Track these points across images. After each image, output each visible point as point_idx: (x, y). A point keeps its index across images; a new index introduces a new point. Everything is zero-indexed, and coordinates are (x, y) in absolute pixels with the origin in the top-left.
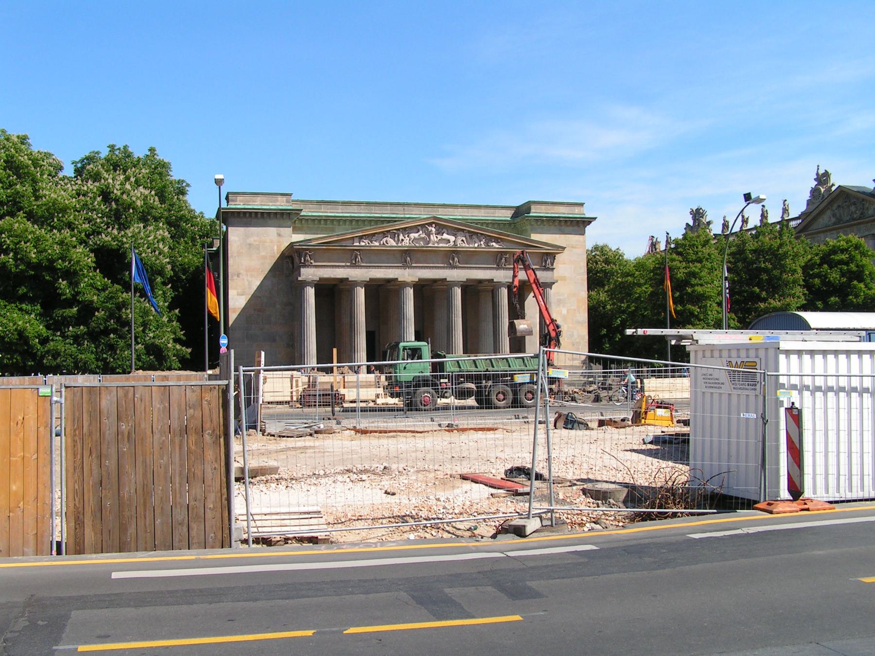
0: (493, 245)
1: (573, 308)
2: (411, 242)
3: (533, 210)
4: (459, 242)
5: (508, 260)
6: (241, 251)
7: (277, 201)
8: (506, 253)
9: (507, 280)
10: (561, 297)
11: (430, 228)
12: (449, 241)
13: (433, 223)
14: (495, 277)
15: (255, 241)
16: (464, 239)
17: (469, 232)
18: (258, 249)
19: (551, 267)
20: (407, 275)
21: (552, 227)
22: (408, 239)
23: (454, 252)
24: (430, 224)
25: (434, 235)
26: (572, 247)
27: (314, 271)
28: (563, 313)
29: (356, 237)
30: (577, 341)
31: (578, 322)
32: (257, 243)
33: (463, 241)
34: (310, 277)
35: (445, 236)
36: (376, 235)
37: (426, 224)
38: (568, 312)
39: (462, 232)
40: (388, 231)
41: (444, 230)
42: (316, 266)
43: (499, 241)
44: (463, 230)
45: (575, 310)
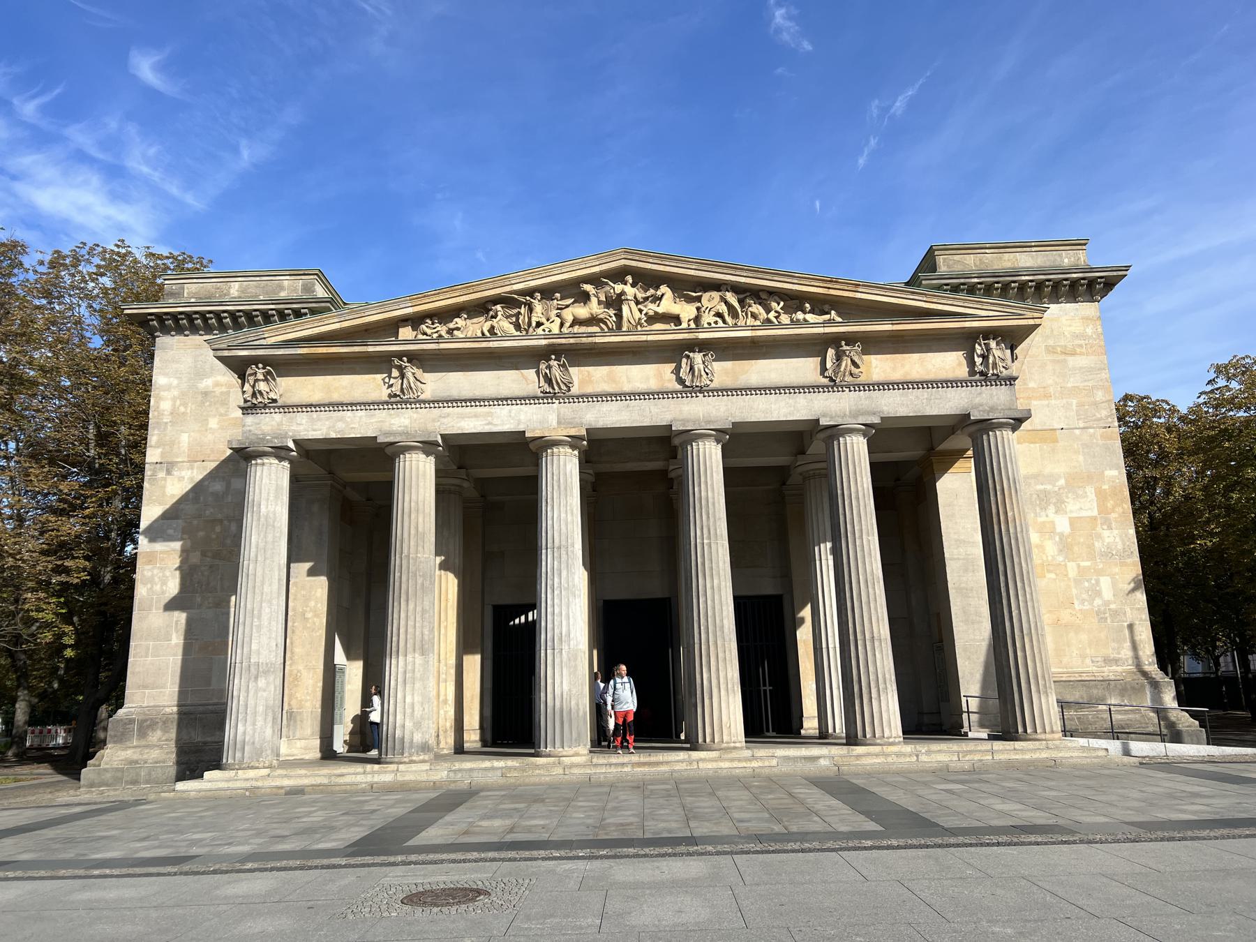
1: (1089, 514)
3: (943, 268)
4: (707, 318)
6: (182, 409)
7: (282, 288)
8: (851, 339)
9: (862, 420)
10: (1049, 487)
11: (619, 288)
12: (676, 319)
14: (824, 416)
15: (217, 384)
16: (723, 308)
17: (737, 289)
18: (224, 403)
19: (1005, 373)
20: (555, 423)
22: (558, 321)
25: (633, 304)
26: (1063, 353)
27: (280, 424)
30: (1113, 606)
31: (1108, 554)
32: (224, 389)
33: (719, 315)
35: (669, 303)
38: (1072, 524)
40: (497, 300)
41: (664, 289)
42: (287, 408)
44: (717, 286)
45: (1095, 518)
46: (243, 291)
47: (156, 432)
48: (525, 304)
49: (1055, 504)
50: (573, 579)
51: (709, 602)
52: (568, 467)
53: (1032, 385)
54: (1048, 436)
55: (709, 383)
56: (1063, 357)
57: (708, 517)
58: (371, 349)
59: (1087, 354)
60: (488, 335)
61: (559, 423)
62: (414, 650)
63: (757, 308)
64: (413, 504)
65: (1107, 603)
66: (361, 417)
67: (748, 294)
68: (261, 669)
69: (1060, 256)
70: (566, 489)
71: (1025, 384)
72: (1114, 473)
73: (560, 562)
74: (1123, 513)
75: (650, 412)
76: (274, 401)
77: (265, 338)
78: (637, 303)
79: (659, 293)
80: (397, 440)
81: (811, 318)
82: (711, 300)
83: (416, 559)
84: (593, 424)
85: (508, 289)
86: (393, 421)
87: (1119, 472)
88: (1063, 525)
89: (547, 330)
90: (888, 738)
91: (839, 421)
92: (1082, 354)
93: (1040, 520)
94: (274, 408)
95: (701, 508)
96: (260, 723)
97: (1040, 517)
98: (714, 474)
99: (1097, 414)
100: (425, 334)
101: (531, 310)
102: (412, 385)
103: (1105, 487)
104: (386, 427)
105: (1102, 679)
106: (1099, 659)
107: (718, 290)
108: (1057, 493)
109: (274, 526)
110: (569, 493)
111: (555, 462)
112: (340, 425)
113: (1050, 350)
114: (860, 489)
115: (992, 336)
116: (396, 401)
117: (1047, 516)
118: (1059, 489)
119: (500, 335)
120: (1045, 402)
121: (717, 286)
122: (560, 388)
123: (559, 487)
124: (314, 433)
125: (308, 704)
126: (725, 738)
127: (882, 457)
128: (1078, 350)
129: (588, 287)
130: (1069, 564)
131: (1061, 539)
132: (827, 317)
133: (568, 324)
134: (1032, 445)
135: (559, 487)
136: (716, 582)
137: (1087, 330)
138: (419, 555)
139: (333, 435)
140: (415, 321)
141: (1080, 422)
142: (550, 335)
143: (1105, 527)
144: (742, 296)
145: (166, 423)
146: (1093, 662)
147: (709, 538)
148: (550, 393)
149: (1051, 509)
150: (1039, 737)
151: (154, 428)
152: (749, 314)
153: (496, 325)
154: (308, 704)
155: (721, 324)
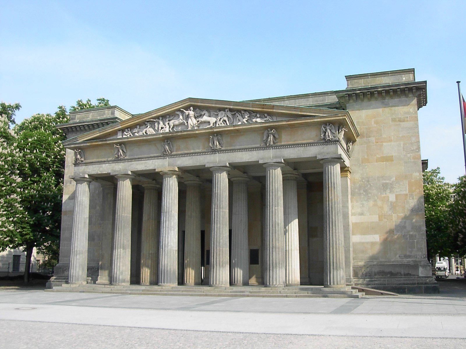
0: (256, 122)
1: (405, 192)
2: (171, 129)
5: (277, 136)
8: (271, 128)
13: (192, 106)
14: (262, 159)
16: (226, 118)
17: (231, 110)
19: (334, 139)
21: (373, 102)
23: (213, 134)
24: (187, 108)
25: (193, 119)
26: (400, 121)
27: (84, 169)
28: (390, 200)
29: (119, 130)
30: (411, 233)
34: (81, 174)
36: (138, 127)
37: (183, 108)
39: (223, 112)
42: (86, 164)
43: (266, 115)
44: (224, 109)
46: (93, 116)
47: (67, 169)
48: (157, 122)
49: (390, 189)
50: (171, 224)
51: (215, 233)
52: (171, 182)
53: (384, 136)
54: (389, 159)
55: (220, 147)
56: (399, 123)
57: (218, 200)
58: (108, 142)
59: (410, 121)
60: (145, 134)
61: (168, 165)
62: (121, 248)
63: (240, 117)
64: (121, 196)
65: (409, 231)
66: (107, 166)
67: (236, 112)
68: (78, 252)
69: (402, 77)
70: (170, 190)
71: (381, 136)
72: (417, 174)
73: (166, 218)
74: (419, 192)
75: (200, 160)
76: (82, 161)
77: (78, 140)
78: (195, 118)
79: (203, 113)
80: (116, 174)
81: (259, 120)
82: (221, 114)
83: (122, 216)
84: (180, 165)
85: (150, 117)
86: (116, 167)
87: (419, 174)
88: (392, 198)
89: (164, 131)
90: (275, 285)
91: (266, 161)
92: (407, 121)
93: (383, 196)
94: (83, 164)
95: (215, 197)
96: (77, 270)
97: (383, 194)
98: (221, 184)
99: (412, 148)
100: (125, 135)
101: (159, 123)
102: (122, 154)
103: (413, 181)
104: (114, 169)
105: (401, 264)
106: (403, 256)
107: (225, 111)
108: (391, 184)
109: (82, 205)
110: (171, 192)
111: (166, 180)
112: (101, 169)
113: (394, 120)
114: (274, 188)
115: (328, 124)
116: (118, 160)
117: (386, 194)
118: (392, 182)
119: (148, 134)
120: (389, 143)
121: (224, 109)
122: (168, 152)
123: (167, 190)
124: (94, 172)
125: (107, 265)
126: (217, 283)
127: (285, 176)
128: (406, 119)
129: (178, 113)
130: (393, 215)
131: (391, 204)
132: (266, 119)
133: (172, 127)
134: (382, 163)
135: (167, 190)
136: (218, 225)
137: (411, 110)
138: (123, 215)
139: (99, 173)
140: (123, 130)
141: (404, 152)
142: (166, 133)
143: (411, 198)
144: (233, 113)
145: (70, 166)
146: (399, 256)
147: (217, 209)
148: (165, 154)
149: (388, 191)
150: (331, 286)
151: (66, 167)
152: (238, 120)
153: (147, 130)
154: (107, 265)
155: (223, 125)
